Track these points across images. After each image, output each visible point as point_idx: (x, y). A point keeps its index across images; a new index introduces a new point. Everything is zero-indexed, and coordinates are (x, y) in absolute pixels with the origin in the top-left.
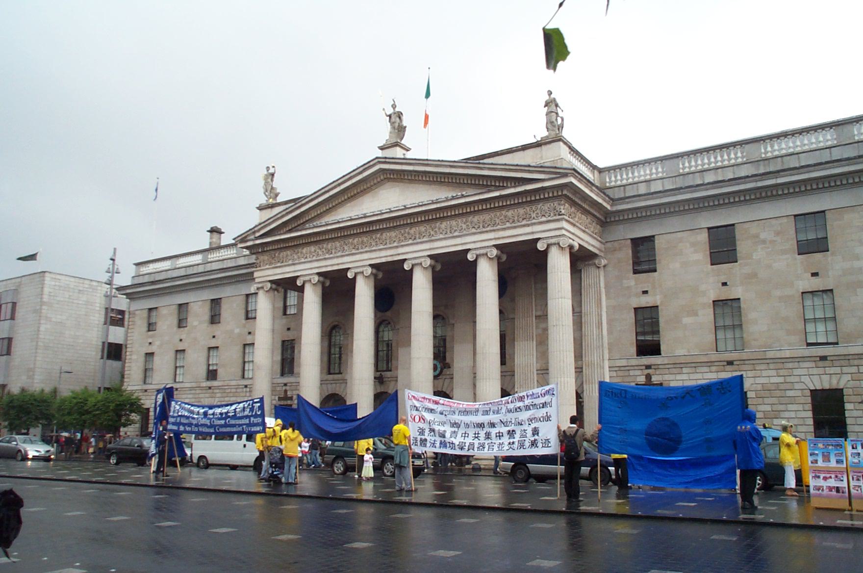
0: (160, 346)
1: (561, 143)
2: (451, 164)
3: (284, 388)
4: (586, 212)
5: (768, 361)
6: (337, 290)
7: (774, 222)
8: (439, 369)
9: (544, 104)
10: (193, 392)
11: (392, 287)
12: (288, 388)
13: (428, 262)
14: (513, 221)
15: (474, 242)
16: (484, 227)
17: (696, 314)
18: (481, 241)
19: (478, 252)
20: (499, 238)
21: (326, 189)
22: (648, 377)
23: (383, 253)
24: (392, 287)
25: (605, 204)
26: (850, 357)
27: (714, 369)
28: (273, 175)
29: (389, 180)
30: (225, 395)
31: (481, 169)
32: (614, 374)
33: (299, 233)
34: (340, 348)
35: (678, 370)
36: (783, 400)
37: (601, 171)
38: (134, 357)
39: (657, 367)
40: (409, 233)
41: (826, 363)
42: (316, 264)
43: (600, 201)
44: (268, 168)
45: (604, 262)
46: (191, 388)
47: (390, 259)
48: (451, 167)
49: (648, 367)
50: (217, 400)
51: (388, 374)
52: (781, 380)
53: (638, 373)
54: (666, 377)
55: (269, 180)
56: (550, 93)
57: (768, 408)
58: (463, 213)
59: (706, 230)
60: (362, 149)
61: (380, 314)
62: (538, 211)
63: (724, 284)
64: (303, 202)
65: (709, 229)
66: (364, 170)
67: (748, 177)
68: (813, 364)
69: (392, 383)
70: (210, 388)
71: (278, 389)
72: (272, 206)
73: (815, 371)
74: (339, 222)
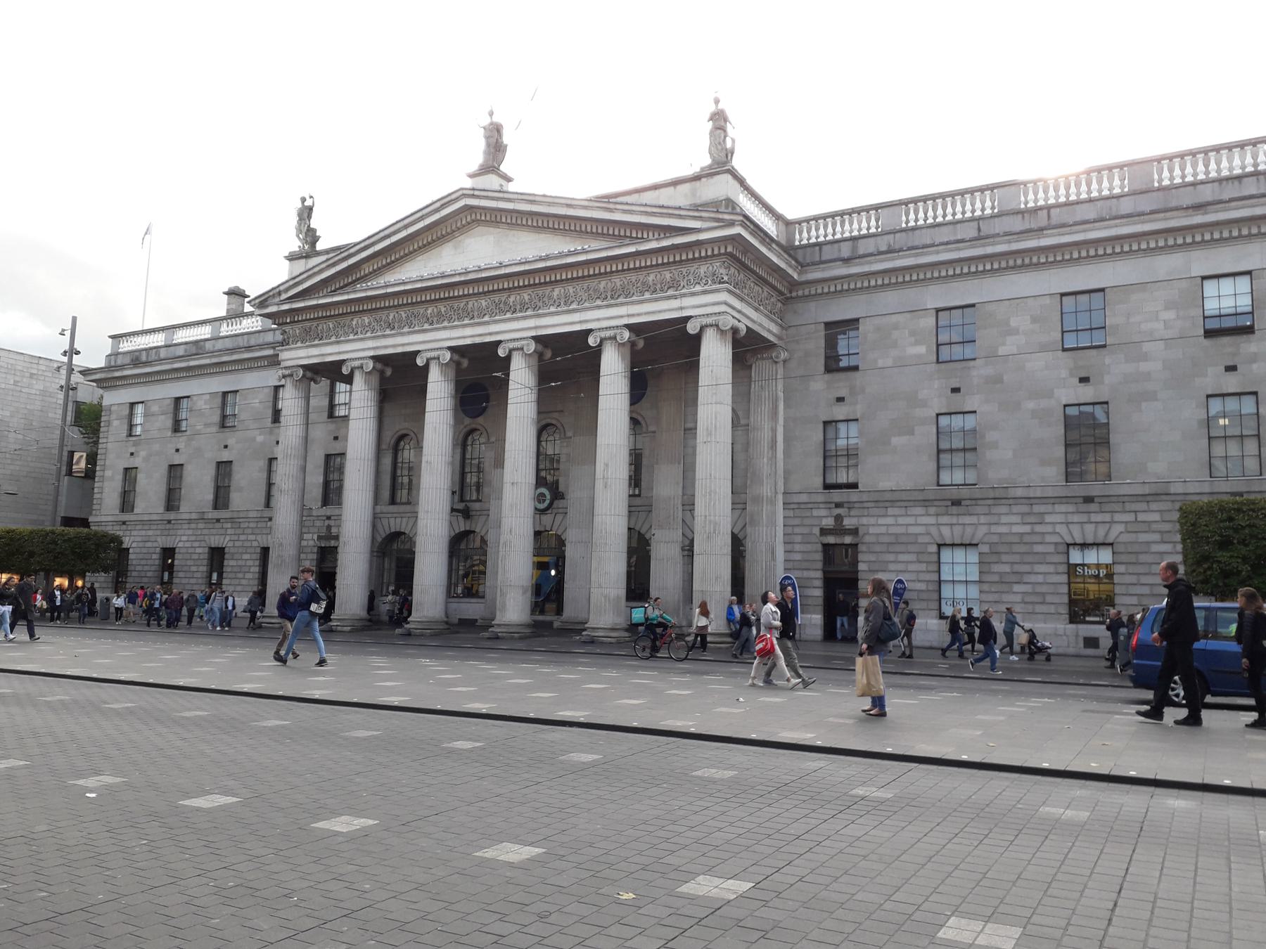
0: (146, 459)
1: (730, 177)
3: (327, 522)
4: (762, 281)
5: (1011, 501)
6: (399, 381)
7: (1030, 301)
8: (547, 502)
9: (708, 116)
10: (193, 526)
11: (480, 379)
12: (332, 523)
13: (532, 347)
14: (655, 291)
15: (598, 320)
16: (612, 298)
17: (912, 433)
18: (606, 318)
19: (603, 334)
20: (633, 315)
21: (387, 232)
22: (838, 518)
23: (469, 331)
24: (480, 379)
25: (790, 271)
26: (1126, 499)
27: (932, 510)
28: (311, 209)
29: (478, 222)
30: (240, 531)
31: (610, 210)
32: (791, 513)
33: (345, 297)
34: (410, 469)
35: (882, 511)
36: (1029, 559)
37: (788, 223)
38: (108, 473)
39: (850, 506)
40: (505, 303)
41: (1093, 507)
42: (370, 344)
43: (783, 265)
44: (303, 200)
45: (784, 355)
46: (190, 521)
47: (478, 340)
49: (838, 505)
50: (228, 538)
51: (477, 506)
52: (1027, 529)
53: (823, 512)
54: (864, 521)
55: (306, 215)
56: (717, 101)
57: (1007, 568)
58: (583, 277)
59: (934, 312)
60: (447, 173)
61: (467, 421)
62: (691, 277)
63: (956, 390)
64: (352, 251)
65: (938, 311)
66: (443, 206)
67: (998, 235)
68: (1071, 508)
69: (483, 519)
70: (218, 520)
71: (318, 523)
72: (307, 256)
73: (1076, 518)
74: (404, 283)
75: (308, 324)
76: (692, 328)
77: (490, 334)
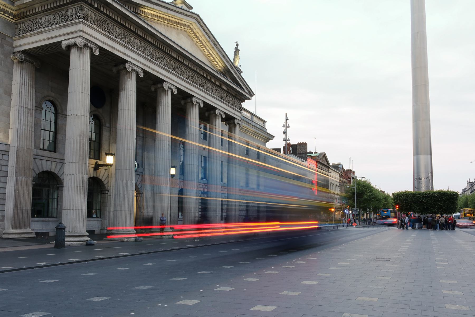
2: (225, 55)
48: (224, 57)
75: (103, 17)
77: (190, 90)
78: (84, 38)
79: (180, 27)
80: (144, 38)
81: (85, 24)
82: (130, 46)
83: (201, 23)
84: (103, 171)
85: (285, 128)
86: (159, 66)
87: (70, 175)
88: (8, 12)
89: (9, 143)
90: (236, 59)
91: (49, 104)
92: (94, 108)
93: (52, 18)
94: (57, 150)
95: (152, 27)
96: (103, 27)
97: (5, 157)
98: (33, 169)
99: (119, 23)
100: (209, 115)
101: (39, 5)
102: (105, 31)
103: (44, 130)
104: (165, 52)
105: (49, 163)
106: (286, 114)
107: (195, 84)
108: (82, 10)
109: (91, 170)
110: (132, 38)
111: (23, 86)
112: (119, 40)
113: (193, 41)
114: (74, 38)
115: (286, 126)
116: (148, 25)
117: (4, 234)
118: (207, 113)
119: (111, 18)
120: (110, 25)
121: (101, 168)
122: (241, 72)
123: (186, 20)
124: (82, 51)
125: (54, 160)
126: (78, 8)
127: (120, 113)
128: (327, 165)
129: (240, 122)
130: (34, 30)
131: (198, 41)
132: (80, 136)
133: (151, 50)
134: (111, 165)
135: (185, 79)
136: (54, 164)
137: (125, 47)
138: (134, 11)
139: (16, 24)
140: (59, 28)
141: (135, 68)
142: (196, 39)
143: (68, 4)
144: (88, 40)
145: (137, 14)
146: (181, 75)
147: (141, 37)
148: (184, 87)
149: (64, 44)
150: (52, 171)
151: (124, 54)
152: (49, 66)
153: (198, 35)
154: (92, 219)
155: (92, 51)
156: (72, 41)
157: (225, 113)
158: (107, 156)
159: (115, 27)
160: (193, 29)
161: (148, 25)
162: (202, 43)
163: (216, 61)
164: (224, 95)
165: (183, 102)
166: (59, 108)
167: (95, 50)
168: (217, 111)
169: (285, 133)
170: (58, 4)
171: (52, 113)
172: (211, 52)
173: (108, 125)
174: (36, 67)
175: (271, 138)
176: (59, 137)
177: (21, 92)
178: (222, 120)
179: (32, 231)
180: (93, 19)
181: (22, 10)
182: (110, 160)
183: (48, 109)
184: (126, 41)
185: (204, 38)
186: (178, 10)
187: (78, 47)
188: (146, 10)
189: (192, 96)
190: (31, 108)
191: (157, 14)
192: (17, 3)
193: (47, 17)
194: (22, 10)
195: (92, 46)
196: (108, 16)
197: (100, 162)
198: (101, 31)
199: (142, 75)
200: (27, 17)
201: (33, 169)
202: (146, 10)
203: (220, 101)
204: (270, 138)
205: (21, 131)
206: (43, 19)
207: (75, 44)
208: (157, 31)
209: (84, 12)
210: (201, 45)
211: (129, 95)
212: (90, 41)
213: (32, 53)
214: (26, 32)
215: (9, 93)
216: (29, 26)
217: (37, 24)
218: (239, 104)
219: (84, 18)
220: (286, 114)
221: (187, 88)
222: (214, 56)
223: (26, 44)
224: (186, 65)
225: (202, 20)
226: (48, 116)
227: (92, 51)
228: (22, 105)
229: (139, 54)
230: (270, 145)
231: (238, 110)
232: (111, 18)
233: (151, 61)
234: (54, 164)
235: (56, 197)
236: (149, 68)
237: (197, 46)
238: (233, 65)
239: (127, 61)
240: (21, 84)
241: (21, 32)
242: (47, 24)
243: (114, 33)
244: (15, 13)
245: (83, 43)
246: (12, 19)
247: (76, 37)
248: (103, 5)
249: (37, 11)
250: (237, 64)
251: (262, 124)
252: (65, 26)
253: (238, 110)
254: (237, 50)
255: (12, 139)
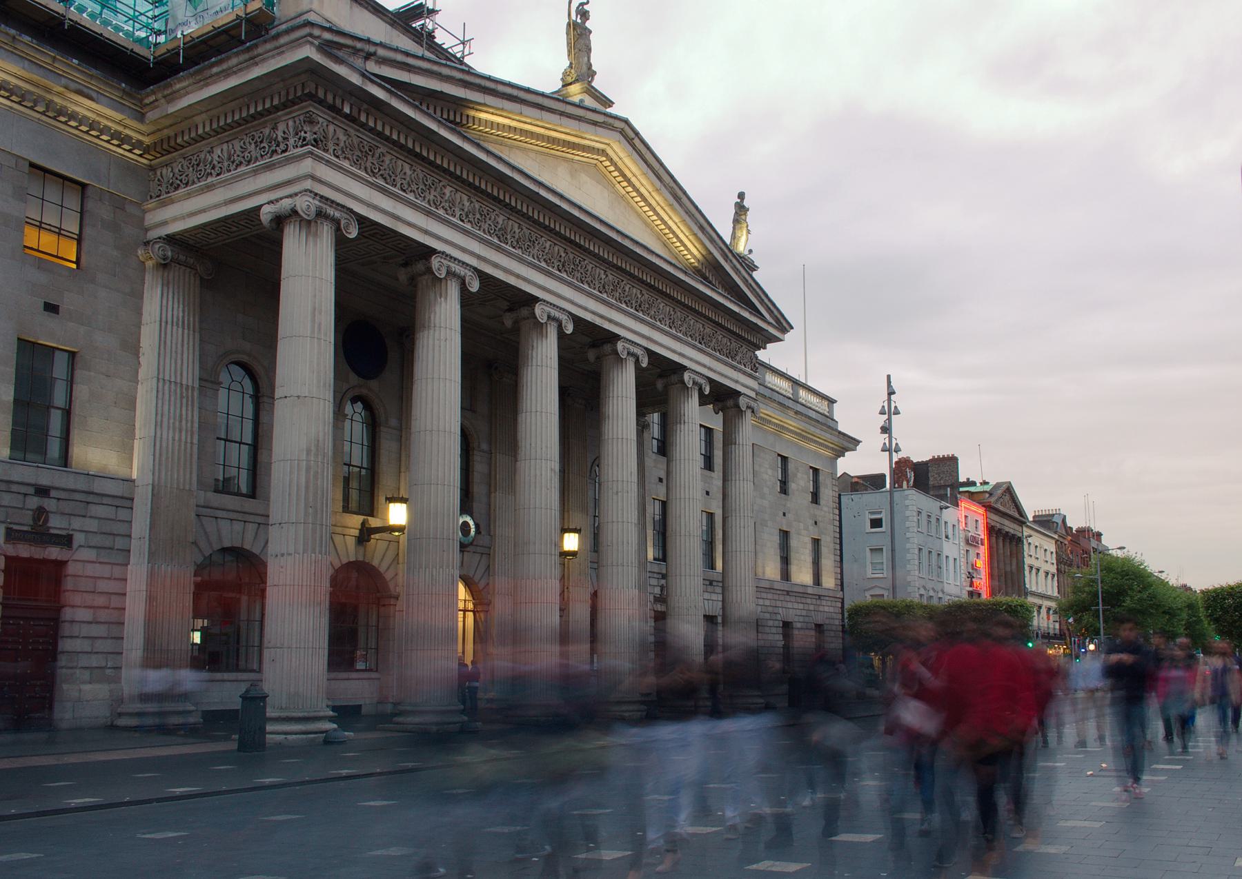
2: (705, 225)
3: (34, 502)
23: (592, 304)
48: (701, 228)
76: (743, 402)
77: (610, 321)
78: (316, 194)
79: (579, 156)
80: (477, 189)
81: (319, 159)
82: (441, 212)
83: (637, 142)
84: (382, 546)
85: (886, 417)
86: (521, 260)
87: (283, 555)
88: (131, 138)
89: (135, 476)
90: (738, 234)
91: (238, 372)
92: (354, 379)
93: (238, 148)
94: (258, 490)
95: (499, 159)
96: (369, 165)
97: (123, 514)
98: (195, 543)
99: (411, 152)
100: (666, 387)
101: (204, 116)
102: (374, 174)
103: (226, 440)
104: (536, 222)
105: (238, 527)
106: (889, 377)
107: (624, 306)
108: (311, 122)
109: (351, 542)
110: (448, 191)
111: (169, 326)
112: (411, 197)
113: (616, 192)
114: (290, 196)
115: (890, 411)
116: (489, 152)
117: (120, 715)
118: (660, 384)
119: (388, 139)
120: (387, 159)
121: (377, 536)
122: (753, 268)
123: (592, 137)
124: (313, 229)
125: (251, 518)
126: (302, 118)
127: (415, 386)
128: (1017, 515)
129: (752, 404)
130: (194, 183)
131: (630, 189)
132: (308, 452)
133: (500, 219)
134: (400, 529)
135: (596, 292)
136: (251, 528)
137: (428, 213)
138: (452, 118)
139: (152, 168)
140: (256, 172)
141: (456, 268)
142: (625, 184)
143: (277, 109)
144: (327, 199)
145: (457, 125)
146: (582, 280)
147: (471, 185)
148: (593, 313)
149: (266, 214)
150: (247, 547)
151: (426, 232)
152: (232, 270)
153: (629, 175)
154: (354, 675)
155: (338, 229)
156: (286, 204)
157: (711, 381)
158: (391, 505)
159: (400, 163)
160: (615, 158)
161: (489, 152)
162: (641, 195)
163: (681, 241)
164: (708, 330)
165: (591, 355)
166: (263, 383)
167: (347, 227)
168: (686, 376)
169: (886, 429)
170: (252, 111)
171: (246, 396)
172: (666, 218)
173: (393, 422)
174: (201, 278)
175: (851, 446)
176: (262, 457)
177: (162, 342)
178: (703, 401)
179: (193, 708)
180: (342, 144)
181: (166, 132)
182: (397, 514)
183: (235, 386)
184: (432, 197)
185: (644, 182)
186: (570, 109)
187: (302, 219)
188: (483, 116)
189: (617, 337)
190: (190, 384)
191: (514, 124)
192: (151, 115)
193: (225, 147)
194: (166, 132)
195: (337, 214)
196: (380, 135)
197: (374, 522)
198: (363, 174)
199: (475, 286)
200: (177, 150)
201: (195, 543)
202: (483, 116)
203: (694, 347)
204: (846, 444)
205: (164, 445)
206: (218, 151)
207: (294, 212)
208: (514, 168)
209: (316, 129)
210: (638, 199)
211: (439, 340)
212: (333, 202)
213: (191, 242)
214: (176, 189)
215: (133, 348)
216: (181, 173)
217: (201, 167)
218: (750, 354)
219: (316, 143)
220: (889, 377)
221: (602, 317)
222: (674, 227)
223: (175, 219)
224: (596, 256)
225: (637, 134)
226: (233, 401)
227: (338, 229)
228: (167, 378)
229: (466, 232)
230: (850, 465)
231: (749, 370)
232: (388, 139)
233: (498, 249)
234: (251, 528)
235: (258, 616)
236: (496, 266)
237: (628, 203)
238: (728, 251)
239: (433, 251)
240: (163, 323)
241: (163, 189)
242: (226, 164)
243: (398, 179)
244: (147, 140)
245: (313, 209)
246: (140, 155)
247: (296, 194)
248: (365, 106)
249: (200, 131)
250: (741, 248)
251: (823, 407)
252: (270, 167)
253: (749, 370)
254: (741, 209)
255: (138, 467)
